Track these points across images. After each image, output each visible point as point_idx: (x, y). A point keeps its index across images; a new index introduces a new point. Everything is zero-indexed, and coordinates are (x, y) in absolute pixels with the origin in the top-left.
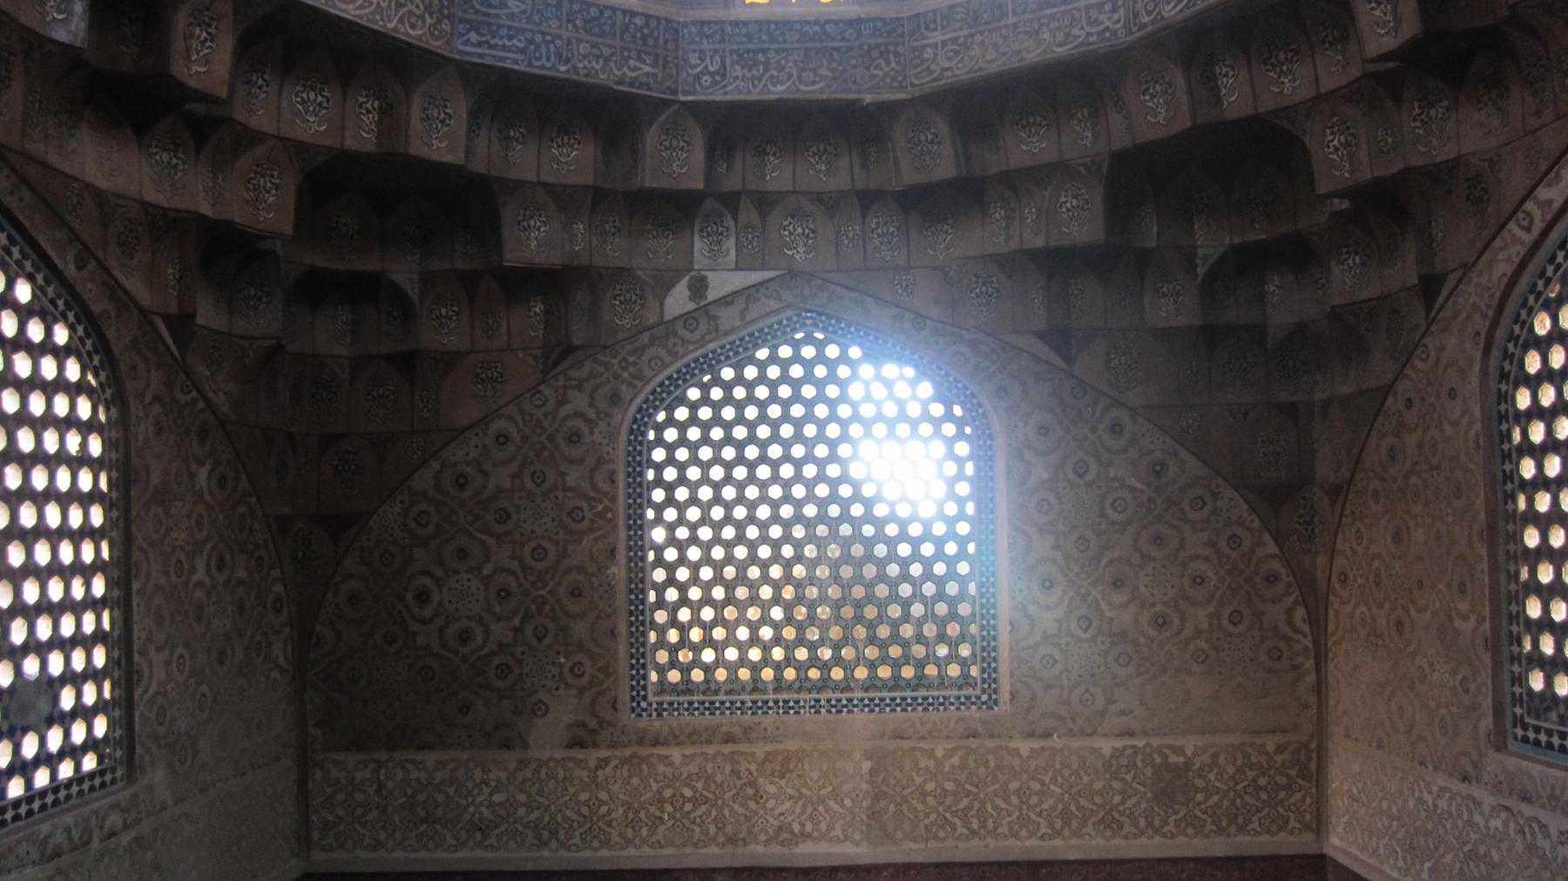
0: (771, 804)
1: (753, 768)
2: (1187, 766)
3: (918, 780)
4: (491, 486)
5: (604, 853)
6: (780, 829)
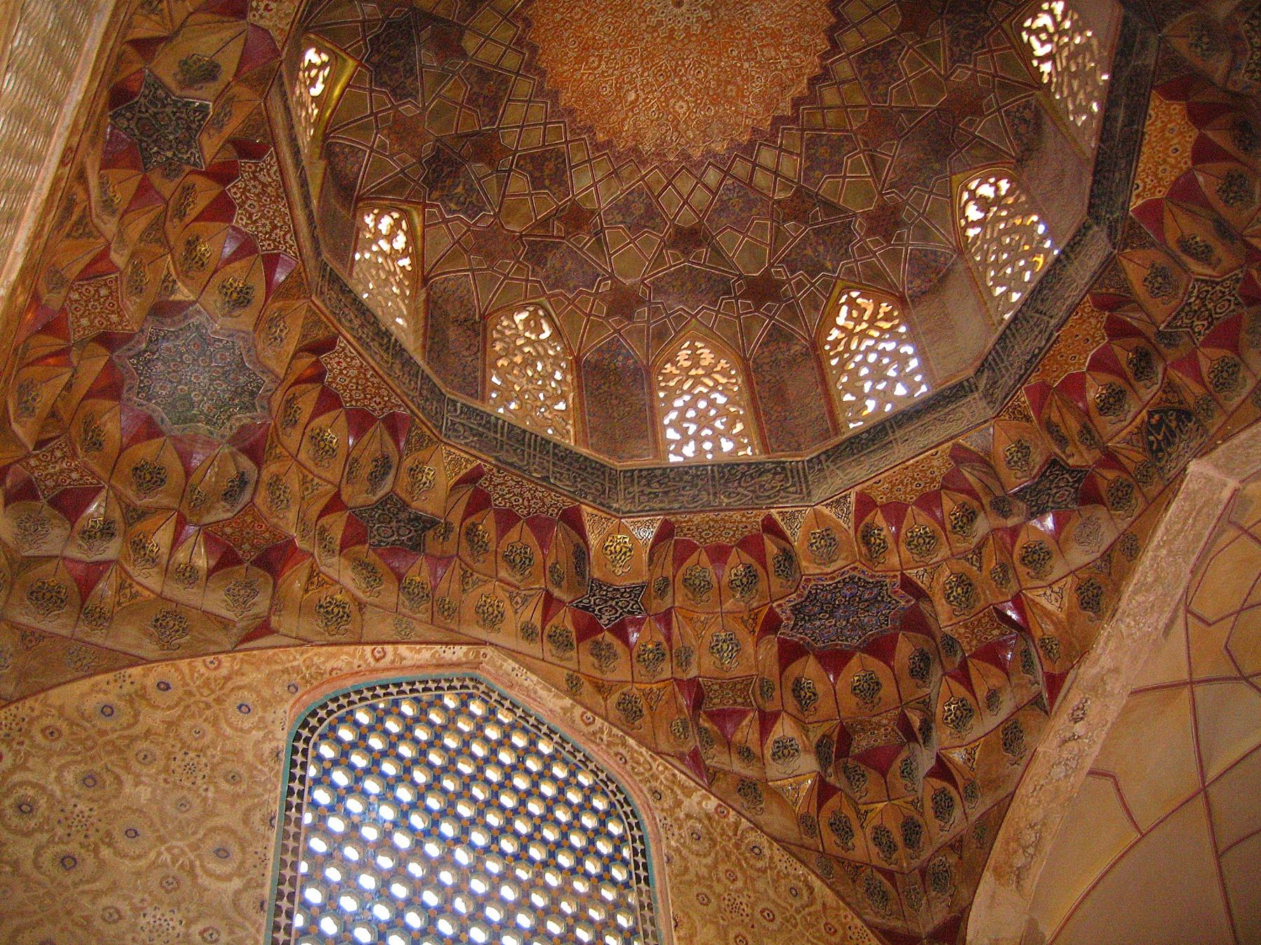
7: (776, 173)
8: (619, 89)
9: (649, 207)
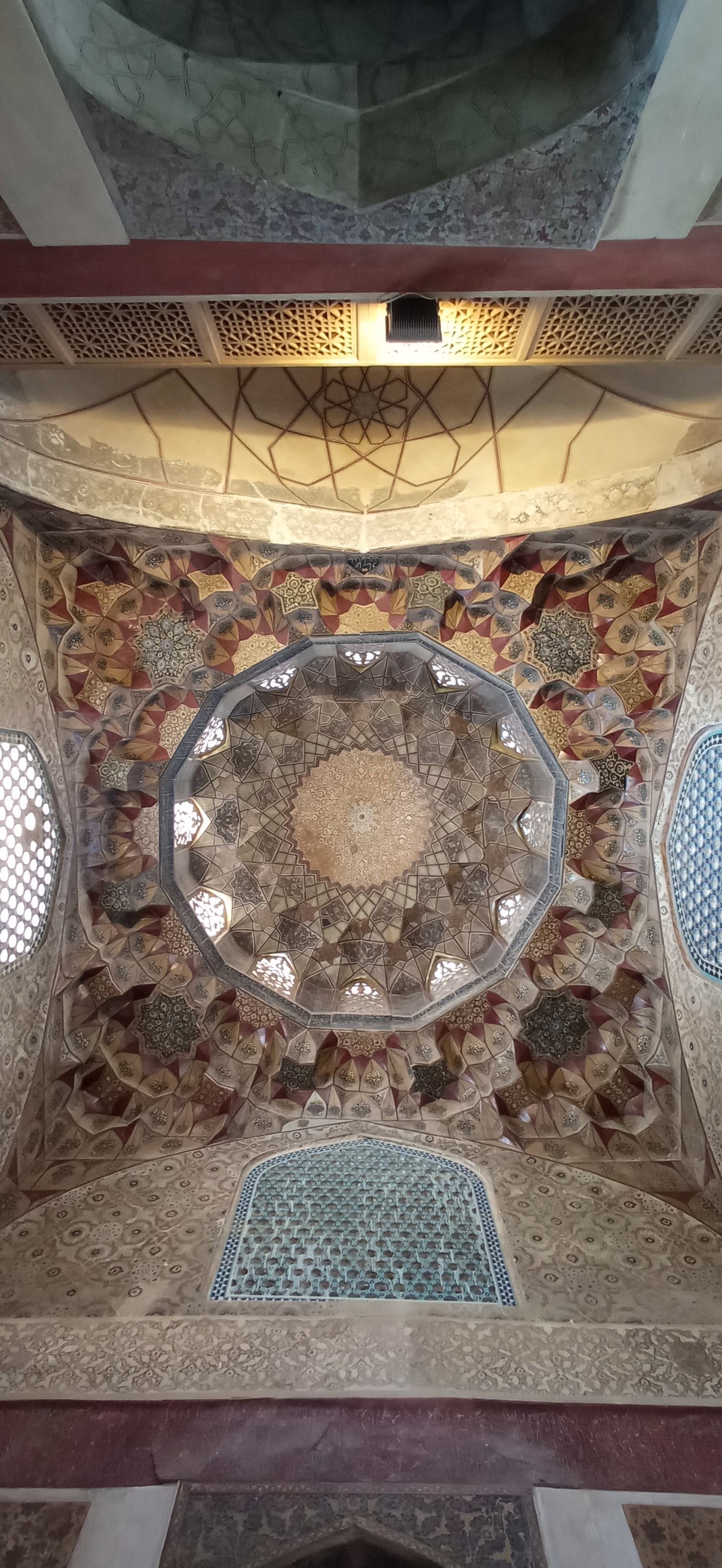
0: (320, 1357)
1: (307, 1332)
3: (456, 1344)
6: (326, 1377)
7: (406, 744)
9: (450, 792)
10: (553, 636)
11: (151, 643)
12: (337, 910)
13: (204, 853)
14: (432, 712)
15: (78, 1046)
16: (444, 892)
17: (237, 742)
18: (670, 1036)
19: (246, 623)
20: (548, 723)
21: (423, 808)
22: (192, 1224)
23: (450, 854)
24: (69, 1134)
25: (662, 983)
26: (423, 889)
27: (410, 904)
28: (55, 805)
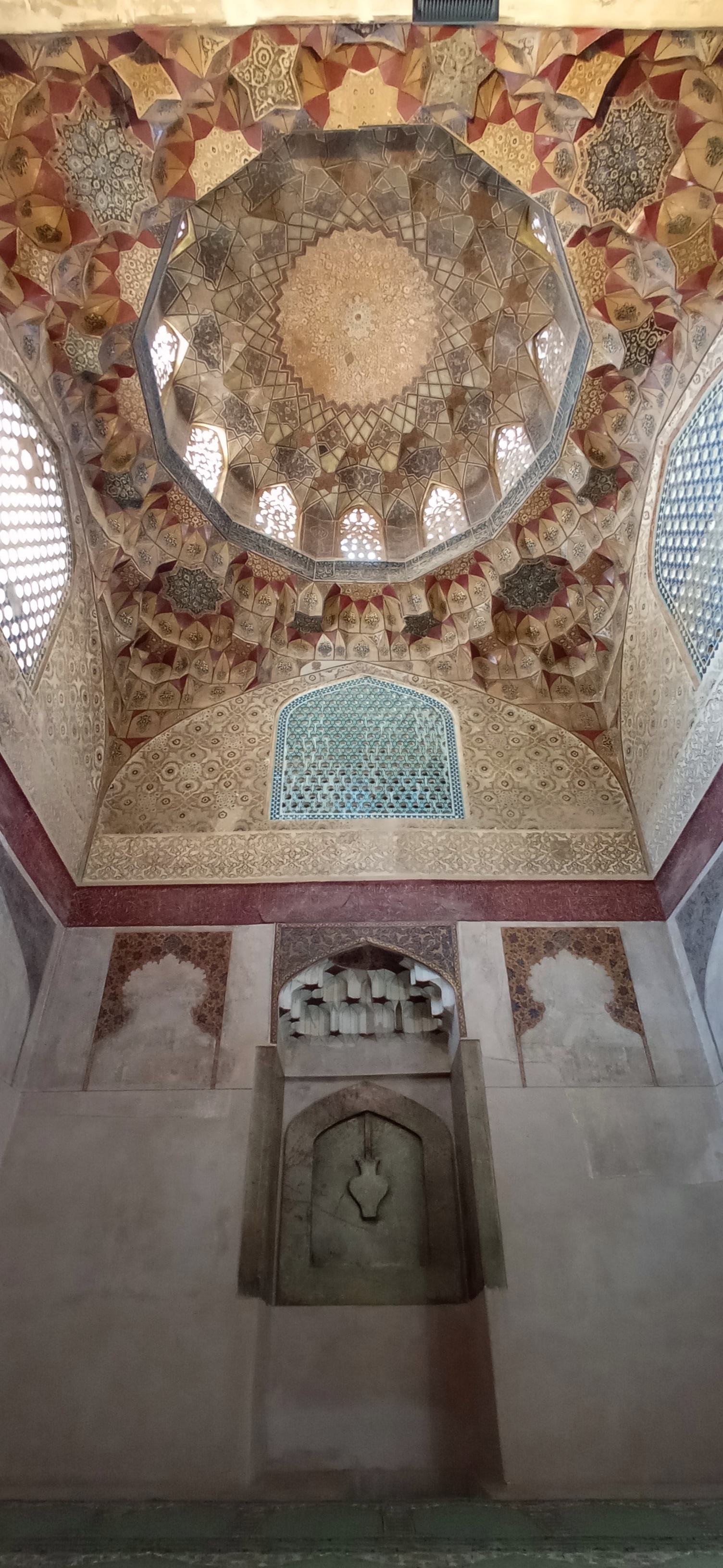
2: (569, 842)
4: (212, 730)
5: (249, 878)
6: (348, 867)
8: (411, 330)
10: (617, 147)
11: (80, 166)
12: (333, 434)
13: (188, 383)
14: (449, 181)
15: (126, 625)
16: (444, 417)
17: (204, 233)
18: (619, 620)
19: (201, 113)
20: (585, 266)
21: (428, 312)
22: (248, 763)
23: (455, 374)
24: (137, 686)
25: (625, 578)
26: (422, 412)
27: (408, 429)
28: (38, 422)
